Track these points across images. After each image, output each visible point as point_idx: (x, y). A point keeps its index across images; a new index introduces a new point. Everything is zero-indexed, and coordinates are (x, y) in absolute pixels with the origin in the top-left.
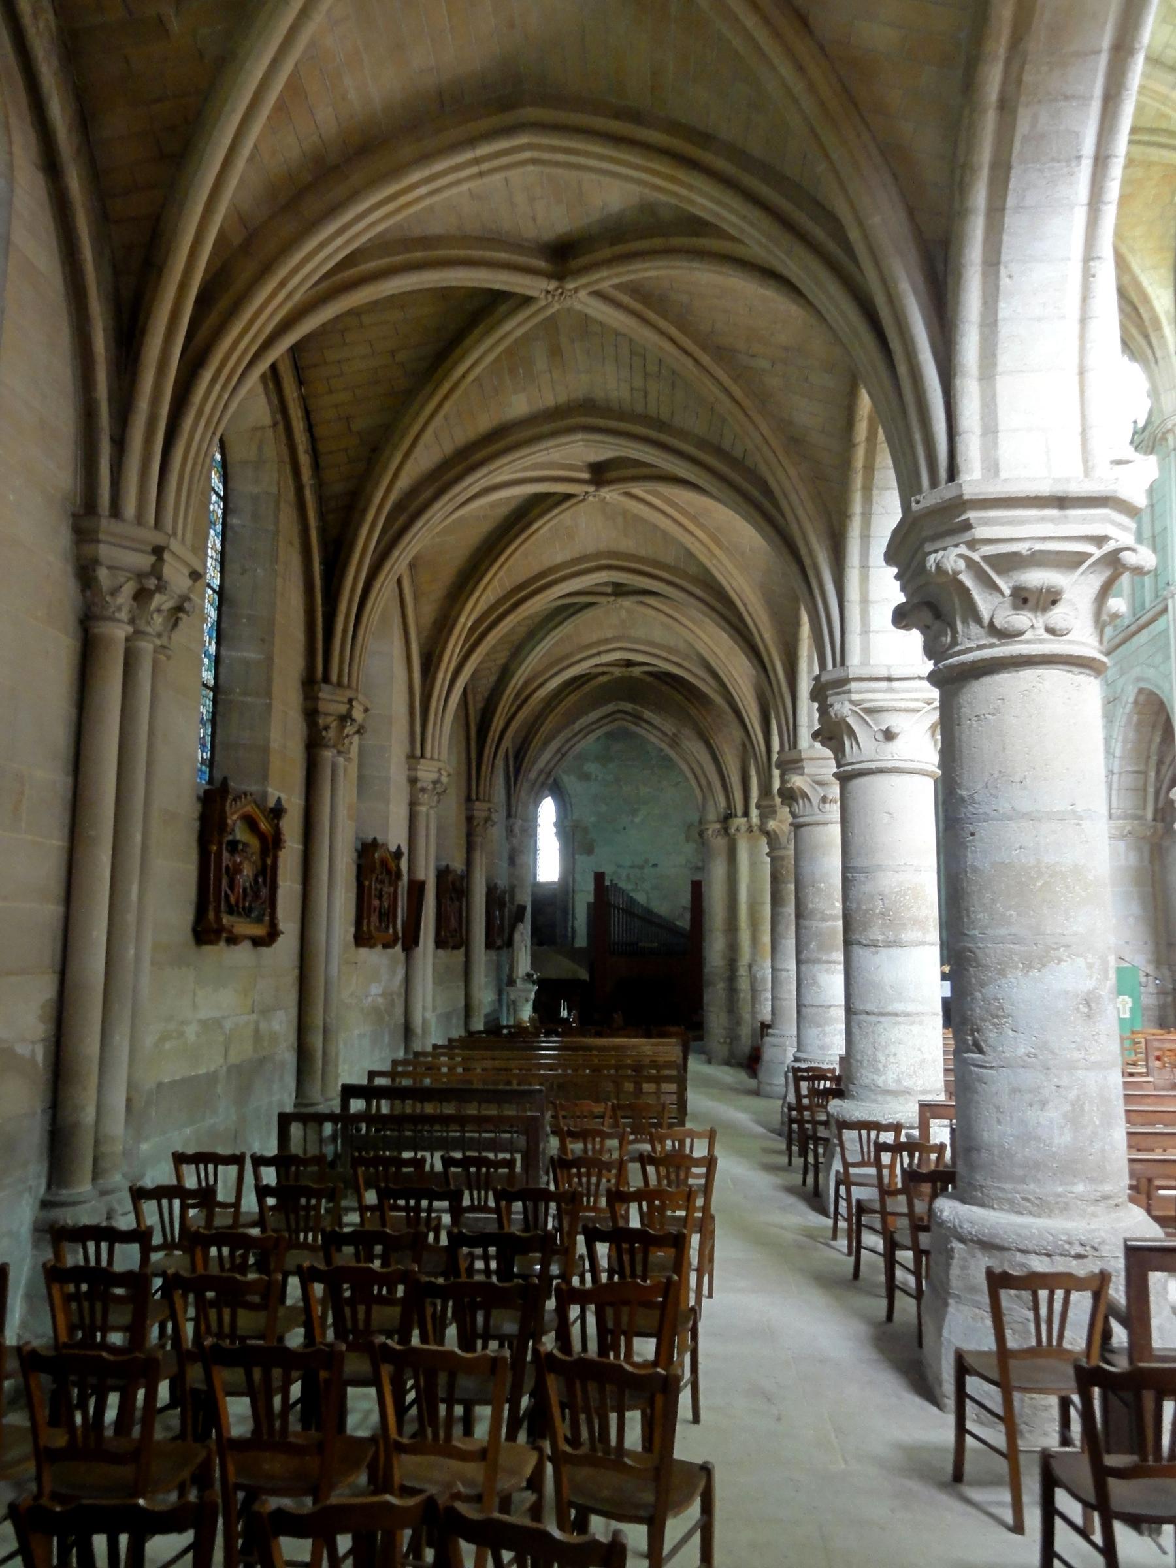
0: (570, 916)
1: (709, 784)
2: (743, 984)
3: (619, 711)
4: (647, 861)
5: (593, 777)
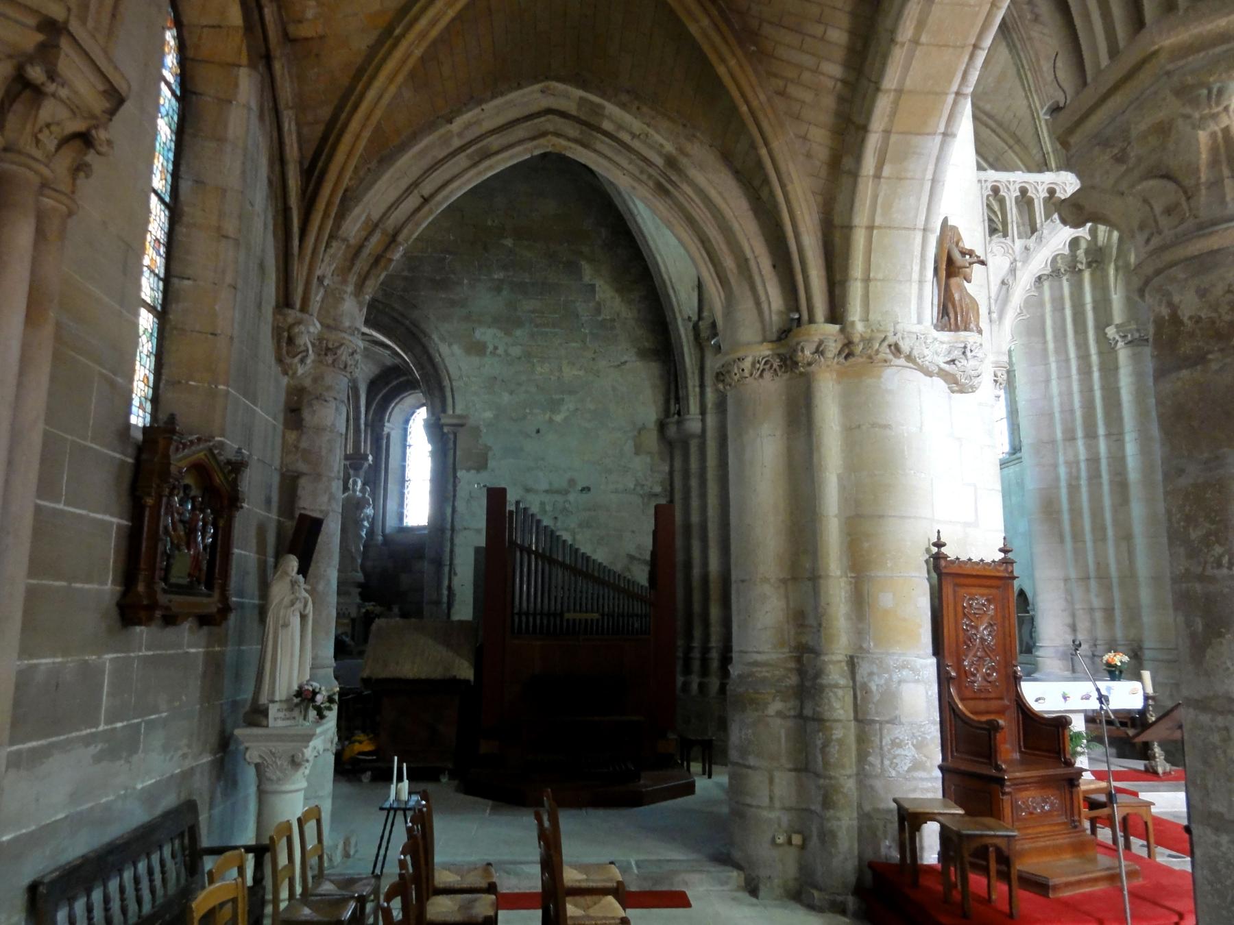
0: (446, 569)
1: (743, 265)
2: (839, 707)
3: (549, 111)
4: (572, 482)
5: (491, 348)
